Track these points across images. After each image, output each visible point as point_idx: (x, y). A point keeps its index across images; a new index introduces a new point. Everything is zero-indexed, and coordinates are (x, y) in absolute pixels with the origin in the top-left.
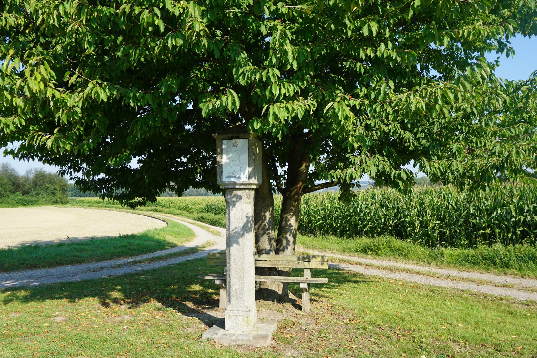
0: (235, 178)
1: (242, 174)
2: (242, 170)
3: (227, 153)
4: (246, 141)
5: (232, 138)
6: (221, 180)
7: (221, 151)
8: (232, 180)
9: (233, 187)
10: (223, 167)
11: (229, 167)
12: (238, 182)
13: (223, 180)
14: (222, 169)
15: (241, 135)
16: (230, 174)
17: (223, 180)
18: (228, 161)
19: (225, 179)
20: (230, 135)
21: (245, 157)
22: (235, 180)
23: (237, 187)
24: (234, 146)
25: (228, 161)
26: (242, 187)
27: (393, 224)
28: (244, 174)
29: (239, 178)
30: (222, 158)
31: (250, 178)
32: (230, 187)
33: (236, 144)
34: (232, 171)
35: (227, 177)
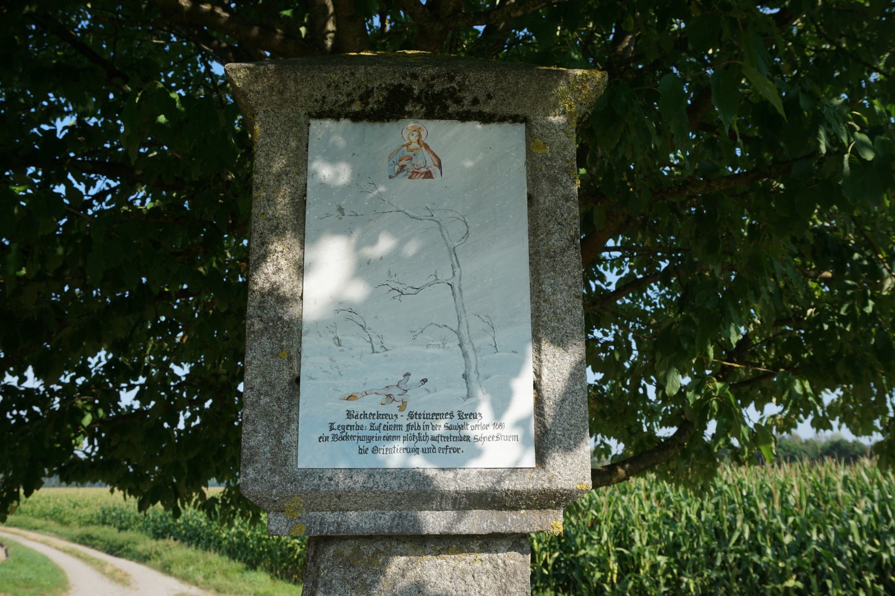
0: (418, 441)
1: (485, 410)
2: (481, 375)
3: (349, 218)
4: (508, 140)
5: (391, 108)
6: (283, 454)
7: (300, 204)
8: (395, 457)
9: (385, 520)
10: (308, 343)
11: (356, 341)
12: (448, 482)
13: (304, 462)
14: (294, 357)
15: (479, 81)
16: (371, 404)
17: (304, 462)
18: (357, 292)
19: (313, 453)
20: (385, 79)
21: (503, 263)
22: (417, 462)
23: (434, 521)
24: (403, 167)
25: (357, 292)
26: (476, 522)
27: (550, 562)
28: (501, 405)
29: (458, 442)
30: (301, 269)
31: (544, 444)
32: (356, 519)
33: (424, 159)
34: (383, 375)
35: (340, 434)
